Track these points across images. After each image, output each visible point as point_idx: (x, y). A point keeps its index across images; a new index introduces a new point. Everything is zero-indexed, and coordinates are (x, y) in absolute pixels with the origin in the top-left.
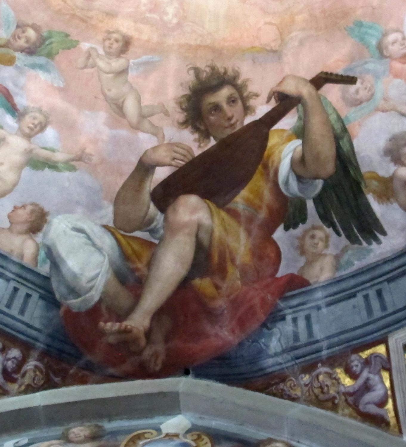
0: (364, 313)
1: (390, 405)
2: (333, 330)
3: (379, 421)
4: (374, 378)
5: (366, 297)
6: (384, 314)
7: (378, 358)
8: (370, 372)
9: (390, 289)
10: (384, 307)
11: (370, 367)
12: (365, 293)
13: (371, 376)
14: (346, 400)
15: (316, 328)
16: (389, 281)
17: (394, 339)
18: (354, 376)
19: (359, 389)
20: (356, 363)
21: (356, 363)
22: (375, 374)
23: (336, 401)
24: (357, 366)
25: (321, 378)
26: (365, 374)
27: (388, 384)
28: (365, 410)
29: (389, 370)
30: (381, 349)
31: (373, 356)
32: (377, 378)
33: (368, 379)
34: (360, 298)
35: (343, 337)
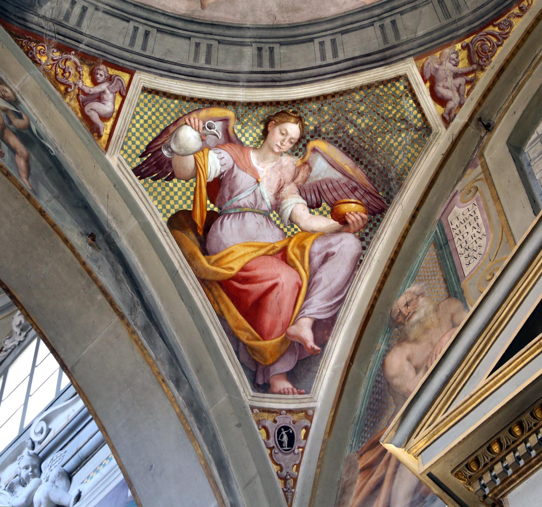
0: (128, 40)
1: (110, 124)
2: (97, 35)
3: (95, 130)
4: (109, 96)
5: (136, 29)
6: (142, 52)
7: (120, 82)
8: (108, 88)
9: (156, 36)
10: (144, 48)
11: (110, 85)
12: (137, 25)
13: (108, 92)
14: (78, 95)
15: (85, 23)
16: (159, 30)
17: (139, 77)
18: (95, 83)
19: (93, 94)
20: (102, 72)
21: (102, 72)
22: (111, 93)
23: (69, 90)
24: (101, 75)
25: (68, 63)
26: (104, 87)
27: (117, 107)
28: (88, 114)
29: (124, 98)
30: (126, 77)
31: (117, 77)
32: (111, 96)
33: (104, 92)
34: (132, 24)
35: (103, 45)
